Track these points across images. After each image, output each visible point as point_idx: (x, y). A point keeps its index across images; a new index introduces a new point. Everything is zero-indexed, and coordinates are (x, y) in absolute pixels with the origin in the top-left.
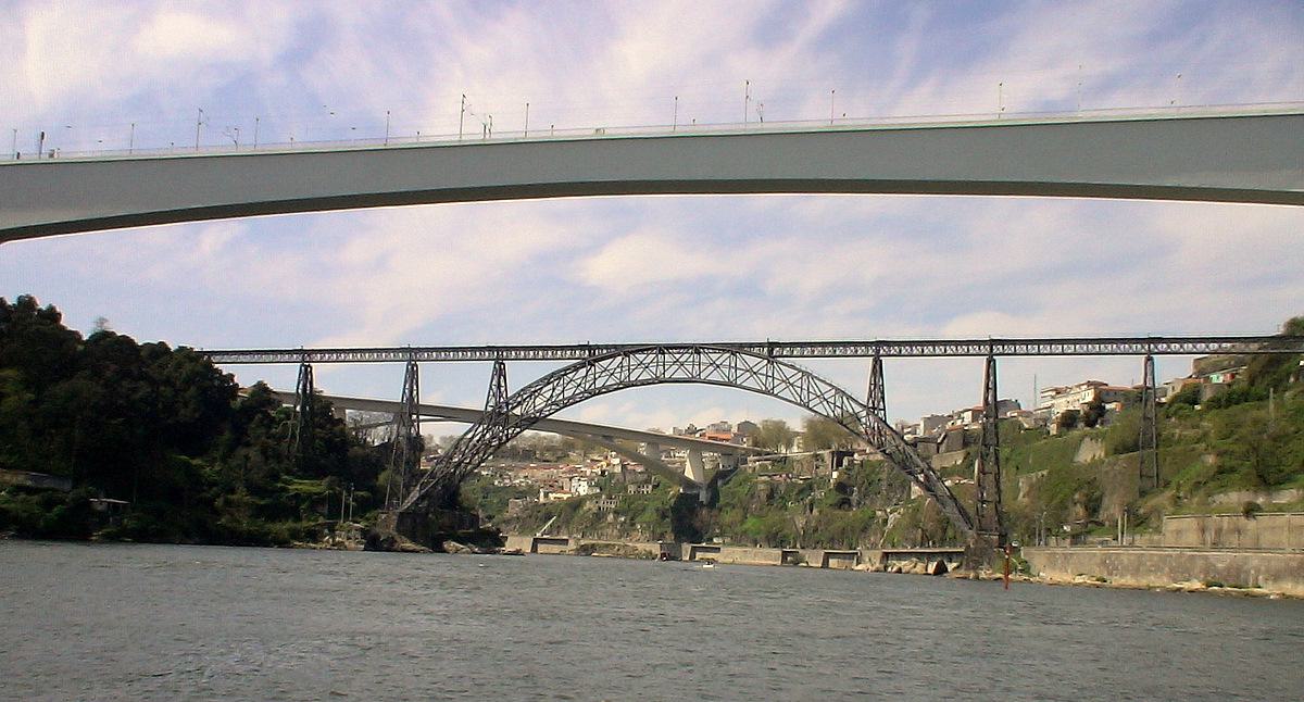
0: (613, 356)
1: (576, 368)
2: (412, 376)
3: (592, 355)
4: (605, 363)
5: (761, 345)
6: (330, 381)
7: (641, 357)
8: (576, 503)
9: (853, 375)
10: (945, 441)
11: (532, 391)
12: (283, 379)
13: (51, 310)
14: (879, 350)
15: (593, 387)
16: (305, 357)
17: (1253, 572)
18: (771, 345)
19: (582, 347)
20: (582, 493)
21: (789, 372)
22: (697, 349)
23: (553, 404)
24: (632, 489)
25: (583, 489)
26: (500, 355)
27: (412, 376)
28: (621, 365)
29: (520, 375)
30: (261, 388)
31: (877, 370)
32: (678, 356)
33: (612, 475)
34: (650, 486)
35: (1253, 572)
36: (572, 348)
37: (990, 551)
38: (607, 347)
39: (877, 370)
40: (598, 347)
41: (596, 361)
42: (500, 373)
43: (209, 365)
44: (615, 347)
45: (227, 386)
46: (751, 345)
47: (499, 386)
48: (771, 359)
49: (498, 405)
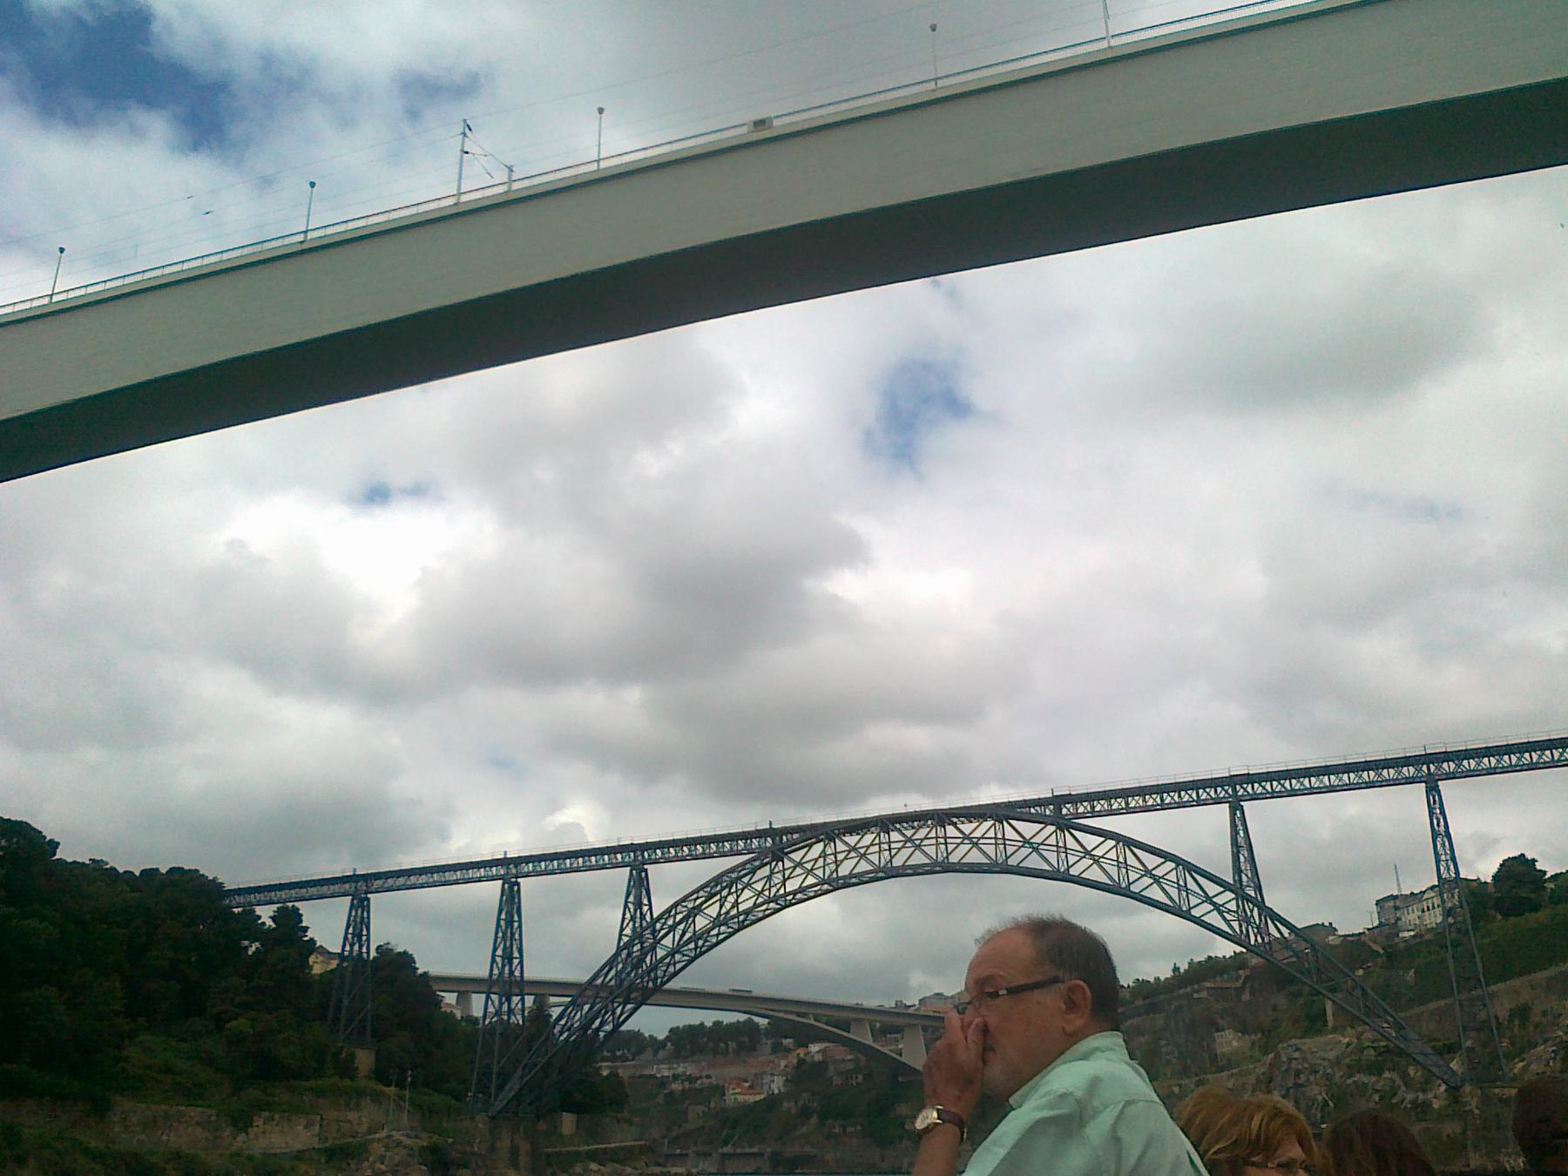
4: (797, 856)
6: (394, 924)
8: (772, 1102)
11: (688, 906)
14: (1234, 790)
16: (358, 889)
18: (1058, 801)
21: (1090, 841)
23: (725, 924)
25: (777, 1085)
26: (638, 859)
28: (824, 855)
29: (671, 883)
31: (1238, 823)
32: (909, 833)
39: (1238, 823)
42: (639, 885)
47: (639, 905)
48: (1064, 825)
49: (637, 936)
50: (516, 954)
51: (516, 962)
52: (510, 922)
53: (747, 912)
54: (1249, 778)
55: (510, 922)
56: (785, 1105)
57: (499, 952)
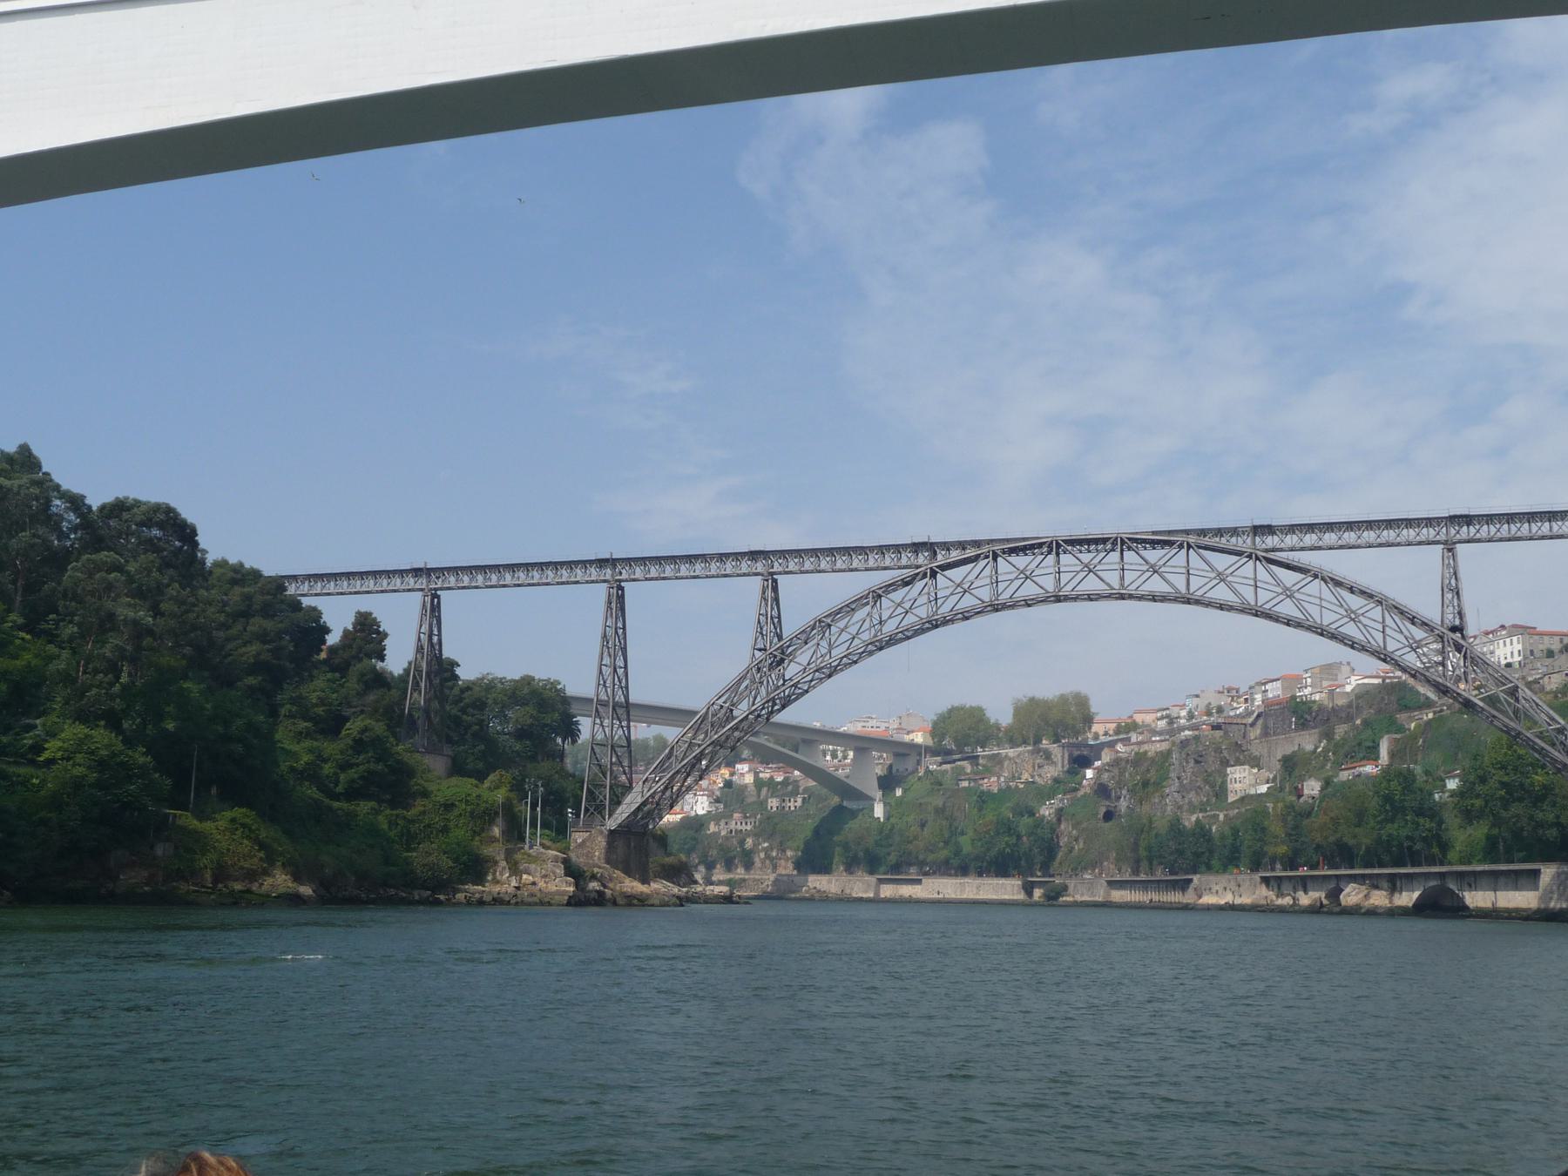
0: (976, 559)
1: (907, 583)
2: (617, 604)
3: (930, 558)
4: (957, 574)
5: (1234, 532)
7: (1021, 561)
9: (1410, 575)
10: (1260, 722)
13: (25, 450)
16: (430, 580)
19: (917, 547)
20: (700, 812)
27: (617, 604)
29: (806, 596)
32: (1086, 557)
34: (799, 800)
36: (898, 548)
38: (962, 545)
40: (947, 546)
41: (944, 567)
44: (977, 544)
46: (1219, 532)
54: (1468, 520)
56: (712, 828)
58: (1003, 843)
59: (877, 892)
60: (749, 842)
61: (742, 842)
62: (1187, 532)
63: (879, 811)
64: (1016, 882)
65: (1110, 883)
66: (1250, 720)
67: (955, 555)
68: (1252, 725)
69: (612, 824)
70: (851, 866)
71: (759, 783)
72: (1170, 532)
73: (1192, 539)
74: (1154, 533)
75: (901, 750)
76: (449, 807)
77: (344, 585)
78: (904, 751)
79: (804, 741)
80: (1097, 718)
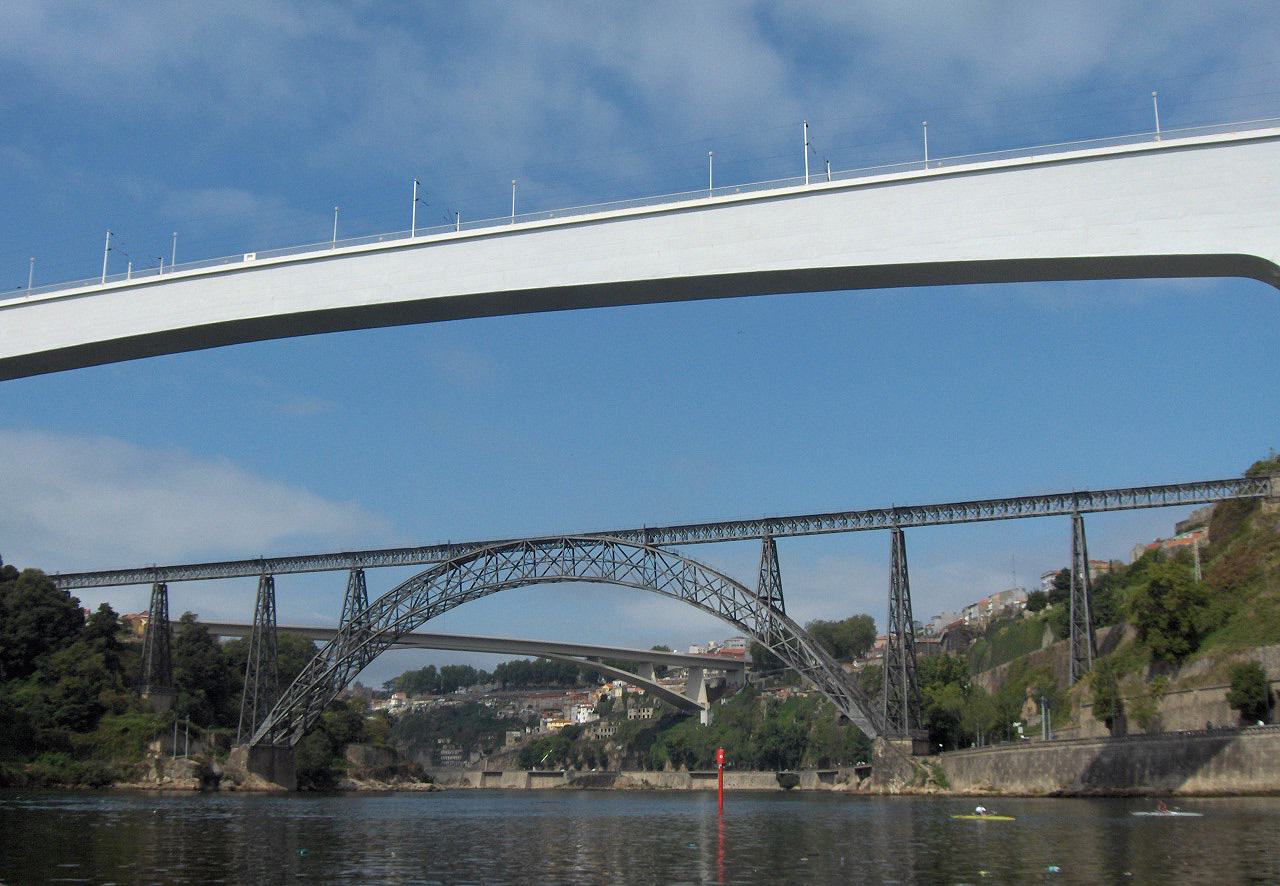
0: (475, 558)
3: (457, 556)
6: (190, 600)
10: (946, 641)
12: (131, 602)
14: (771, 529)
15: (458, 590)
16: (160, 576)
17: (1138, 766)
18: (650, 532)
19: (443, 548)
20: (582, 721)
22: (569, 543)
24: (632, 713)
25: (583, 716)
26: (357, 562)
29: (381, 581)
30: (105, 609)
33: (613, 700)
34: (651, 710)
35: (1138, 766)
37: (900, 761)
38: (470, 546)
40: (461, 546)
43: (53, 587)
44: (479, 545)
45: (72, 614)
47: (358, 598)
50: (363, 596)
51: (362, 600)
52: (266, 607)
53: (435, 606)
55: (266, 607)
57: (351, 594)
58: (771, 743)
59: (690, 786)
60: (608, 747)
61: (602, 748)
62: (607, 534)
63: (704, 718)
64: (771, 775)
65: (820, 775)
66: (939, 640)
67: (468, 552)
68: (942, 643)
69: (254, 741)
70: (676, 765)
71: (625, 695)
72: (596, 534)
73: (609, 538)
74: (586, 535)
75: (733, 668)
76: (125, 730)
77: (107, 580)
78: (732, 666)
79: (642, 663)
80: (877, 637)
